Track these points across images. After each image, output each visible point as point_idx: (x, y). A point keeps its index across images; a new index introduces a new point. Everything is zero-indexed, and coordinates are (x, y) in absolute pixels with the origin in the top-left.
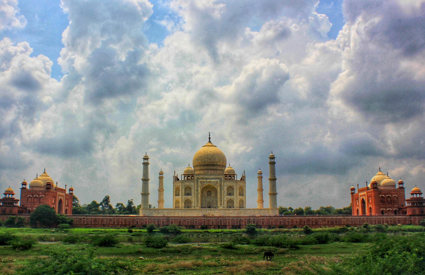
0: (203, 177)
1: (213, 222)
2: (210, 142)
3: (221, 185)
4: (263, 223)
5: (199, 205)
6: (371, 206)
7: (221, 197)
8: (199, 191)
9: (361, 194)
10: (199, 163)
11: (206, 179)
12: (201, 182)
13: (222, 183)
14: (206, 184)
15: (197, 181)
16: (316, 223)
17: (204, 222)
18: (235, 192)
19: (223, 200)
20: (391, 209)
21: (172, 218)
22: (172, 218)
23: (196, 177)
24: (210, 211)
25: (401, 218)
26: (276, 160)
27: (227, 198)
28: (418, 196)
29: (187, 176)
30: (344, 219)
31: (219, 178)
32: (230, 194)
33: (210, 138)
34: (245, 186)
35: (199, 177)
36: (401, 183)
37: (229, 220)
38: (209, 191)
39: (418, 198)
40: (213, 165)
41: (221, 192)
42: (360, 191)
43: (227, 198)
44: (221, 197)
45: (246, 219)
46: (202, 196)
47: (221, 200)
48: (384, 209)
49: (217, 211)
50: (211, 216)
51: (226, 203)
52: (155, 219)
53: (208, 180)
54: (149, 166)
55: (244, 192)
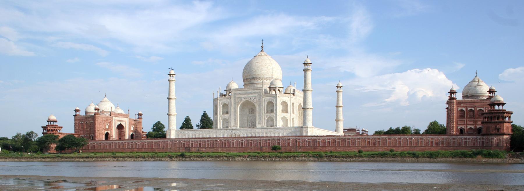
0: (241, 92)
3: (260, 101)
4: (289, 144)
11: (244, 94)
16: (354, 144)
17: (225, 143)
20: (473, 127)
21: (193, 140)
22: (193, 140)
25: (469, 139)
30: (390, 139)
32: (272, 111)
33: (262, 47)
35: (236, 92)
37: (251, 140)
38: (249, 108)
41: (260, 109)
43: (267, 116)
45: (269, 140)
48: (463, 127)
50: (237, 136)
52: (176, 141)
53: (246, 96)
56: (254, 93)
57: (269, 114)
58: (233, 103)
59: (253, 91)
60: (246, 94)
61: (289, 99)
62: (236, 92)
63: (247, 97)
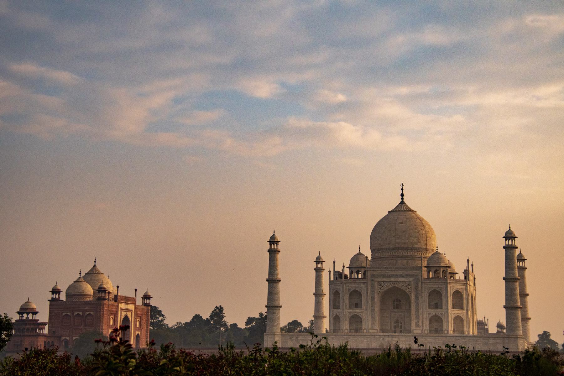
0: (383, 273)
2: (402, 202)
3: (416, 289)
5: (377, 327)
7: (417, 311)
8: (377, 299)
10: (380, 244)
11: (389, 276)
12: (379, 283)
13: (420, 284)
14: (387, 286)
15: (372, 280)
18: (444, 302)
19: (420, 317)
23: (369, 274)
24: (390, 339)
26: (517, 242)
27: (427, 313)
29: (355, 270)
31: (412, 276)
32: (436, 306)
33: (402, 195)
34: (466, 289)
35: (375, 273)
40: (406, 249)
43: (429, 314)
44: (417, 311)
46: (382, 310)
47: (418, 318)
49: (403, 339)
51: (427, 322)
53: (392, 279)
54: (279, 256)
55: (465, 301)
56: (407, 275)
57: (433, 312)
58: (369, 291)
59: (405, 273)
60: (392, 276)
61: (464, 287)
62: (375, 273)
63: (394, 282)
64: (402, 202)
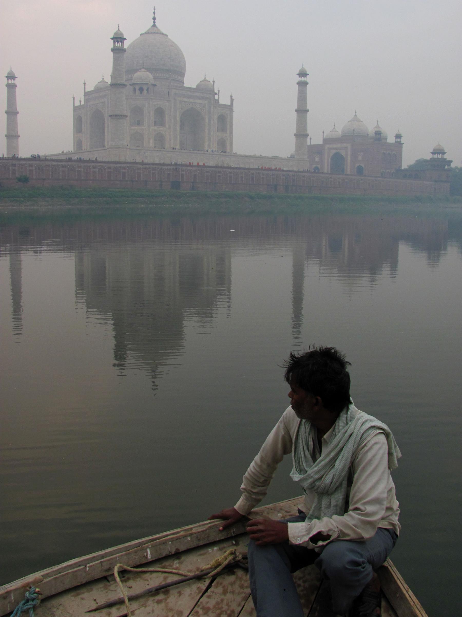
1: (242, 177)
2: (154, 26)
6: (363, 165)
9: (327, 146)
19: (212, 139)
28: (441, 156)
33: (154, 19)
36: (398, 136)
39: (440, 159)
42: (326, 141)
53: (191, 100)
64: (154, 26)
